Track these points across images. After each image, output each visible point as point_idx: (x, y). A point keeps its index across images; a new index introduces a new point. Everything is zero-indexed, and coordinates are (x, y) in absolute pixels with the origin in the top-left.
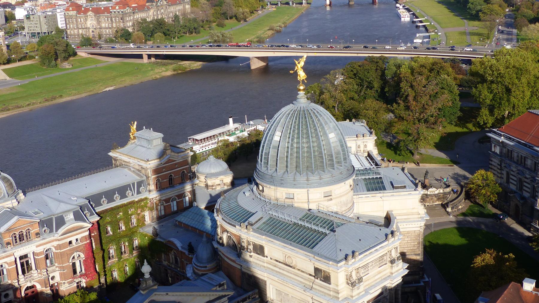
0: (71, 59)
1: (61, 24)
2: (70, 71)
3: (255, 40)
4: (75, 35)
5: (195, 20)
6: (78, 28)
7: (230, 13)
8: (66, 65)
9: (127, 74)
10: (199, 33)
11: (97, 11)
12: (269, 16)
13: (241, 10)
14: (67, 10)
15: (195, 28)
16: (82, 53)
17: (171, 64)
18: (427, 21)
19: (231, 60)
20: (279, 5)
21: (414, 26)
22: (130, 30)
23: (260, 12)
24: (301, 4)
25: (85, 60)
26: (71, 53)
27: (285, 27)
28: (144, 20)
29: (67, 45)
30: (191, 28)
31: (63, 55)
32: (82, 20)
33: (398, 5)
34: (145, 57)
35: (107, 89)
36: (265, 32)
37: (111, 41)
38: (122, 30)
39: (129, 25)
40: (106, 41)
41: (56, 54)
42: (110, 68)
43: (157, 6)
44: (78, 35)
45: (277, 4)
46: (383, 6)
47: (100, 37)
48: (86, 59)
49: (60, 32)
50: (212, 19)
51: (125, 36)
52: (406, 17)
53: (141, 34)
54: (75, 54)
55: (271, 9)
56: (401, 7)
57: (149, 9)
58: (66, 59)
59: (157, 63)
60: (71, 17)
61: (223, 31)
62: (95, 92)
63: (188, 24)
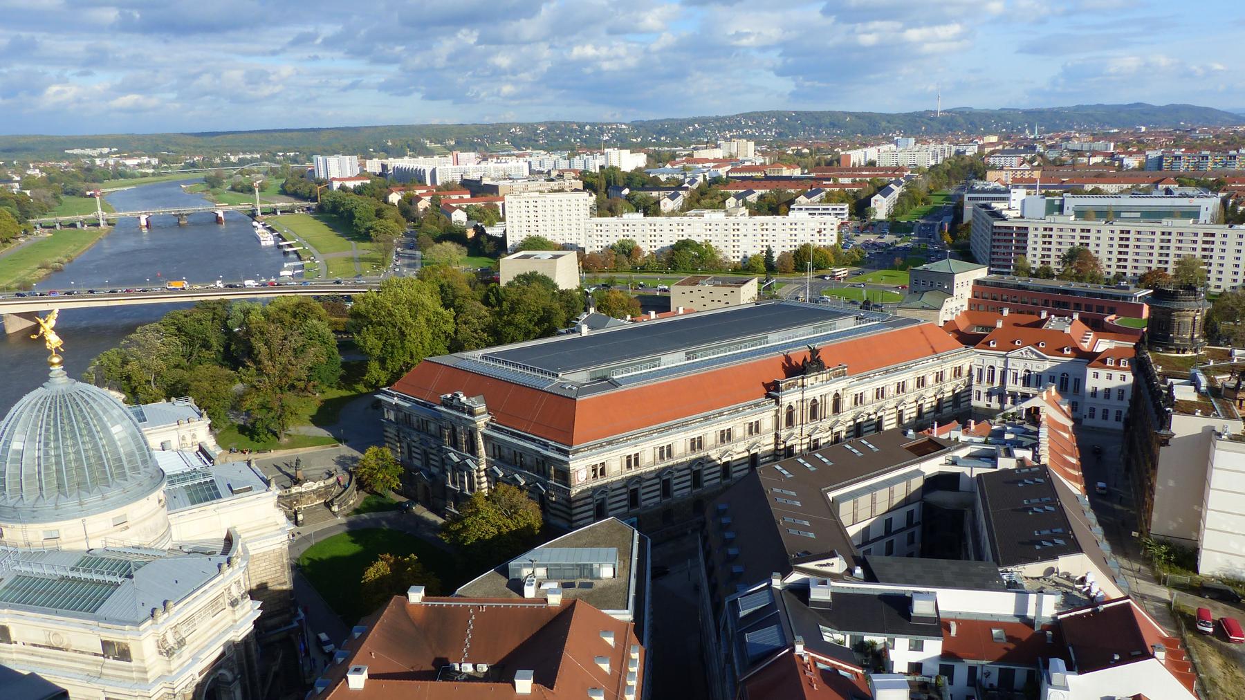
3: (13, 286)
12: (40, 246)
18: (298, 244)
20: (58, 227)
24: (98, 225)
27: (70, 262)
33: (255, 223)
36: (31, 272)
45: (54, 227)
46: (233, 226)
52: (267, 240)
56: (260, 226)
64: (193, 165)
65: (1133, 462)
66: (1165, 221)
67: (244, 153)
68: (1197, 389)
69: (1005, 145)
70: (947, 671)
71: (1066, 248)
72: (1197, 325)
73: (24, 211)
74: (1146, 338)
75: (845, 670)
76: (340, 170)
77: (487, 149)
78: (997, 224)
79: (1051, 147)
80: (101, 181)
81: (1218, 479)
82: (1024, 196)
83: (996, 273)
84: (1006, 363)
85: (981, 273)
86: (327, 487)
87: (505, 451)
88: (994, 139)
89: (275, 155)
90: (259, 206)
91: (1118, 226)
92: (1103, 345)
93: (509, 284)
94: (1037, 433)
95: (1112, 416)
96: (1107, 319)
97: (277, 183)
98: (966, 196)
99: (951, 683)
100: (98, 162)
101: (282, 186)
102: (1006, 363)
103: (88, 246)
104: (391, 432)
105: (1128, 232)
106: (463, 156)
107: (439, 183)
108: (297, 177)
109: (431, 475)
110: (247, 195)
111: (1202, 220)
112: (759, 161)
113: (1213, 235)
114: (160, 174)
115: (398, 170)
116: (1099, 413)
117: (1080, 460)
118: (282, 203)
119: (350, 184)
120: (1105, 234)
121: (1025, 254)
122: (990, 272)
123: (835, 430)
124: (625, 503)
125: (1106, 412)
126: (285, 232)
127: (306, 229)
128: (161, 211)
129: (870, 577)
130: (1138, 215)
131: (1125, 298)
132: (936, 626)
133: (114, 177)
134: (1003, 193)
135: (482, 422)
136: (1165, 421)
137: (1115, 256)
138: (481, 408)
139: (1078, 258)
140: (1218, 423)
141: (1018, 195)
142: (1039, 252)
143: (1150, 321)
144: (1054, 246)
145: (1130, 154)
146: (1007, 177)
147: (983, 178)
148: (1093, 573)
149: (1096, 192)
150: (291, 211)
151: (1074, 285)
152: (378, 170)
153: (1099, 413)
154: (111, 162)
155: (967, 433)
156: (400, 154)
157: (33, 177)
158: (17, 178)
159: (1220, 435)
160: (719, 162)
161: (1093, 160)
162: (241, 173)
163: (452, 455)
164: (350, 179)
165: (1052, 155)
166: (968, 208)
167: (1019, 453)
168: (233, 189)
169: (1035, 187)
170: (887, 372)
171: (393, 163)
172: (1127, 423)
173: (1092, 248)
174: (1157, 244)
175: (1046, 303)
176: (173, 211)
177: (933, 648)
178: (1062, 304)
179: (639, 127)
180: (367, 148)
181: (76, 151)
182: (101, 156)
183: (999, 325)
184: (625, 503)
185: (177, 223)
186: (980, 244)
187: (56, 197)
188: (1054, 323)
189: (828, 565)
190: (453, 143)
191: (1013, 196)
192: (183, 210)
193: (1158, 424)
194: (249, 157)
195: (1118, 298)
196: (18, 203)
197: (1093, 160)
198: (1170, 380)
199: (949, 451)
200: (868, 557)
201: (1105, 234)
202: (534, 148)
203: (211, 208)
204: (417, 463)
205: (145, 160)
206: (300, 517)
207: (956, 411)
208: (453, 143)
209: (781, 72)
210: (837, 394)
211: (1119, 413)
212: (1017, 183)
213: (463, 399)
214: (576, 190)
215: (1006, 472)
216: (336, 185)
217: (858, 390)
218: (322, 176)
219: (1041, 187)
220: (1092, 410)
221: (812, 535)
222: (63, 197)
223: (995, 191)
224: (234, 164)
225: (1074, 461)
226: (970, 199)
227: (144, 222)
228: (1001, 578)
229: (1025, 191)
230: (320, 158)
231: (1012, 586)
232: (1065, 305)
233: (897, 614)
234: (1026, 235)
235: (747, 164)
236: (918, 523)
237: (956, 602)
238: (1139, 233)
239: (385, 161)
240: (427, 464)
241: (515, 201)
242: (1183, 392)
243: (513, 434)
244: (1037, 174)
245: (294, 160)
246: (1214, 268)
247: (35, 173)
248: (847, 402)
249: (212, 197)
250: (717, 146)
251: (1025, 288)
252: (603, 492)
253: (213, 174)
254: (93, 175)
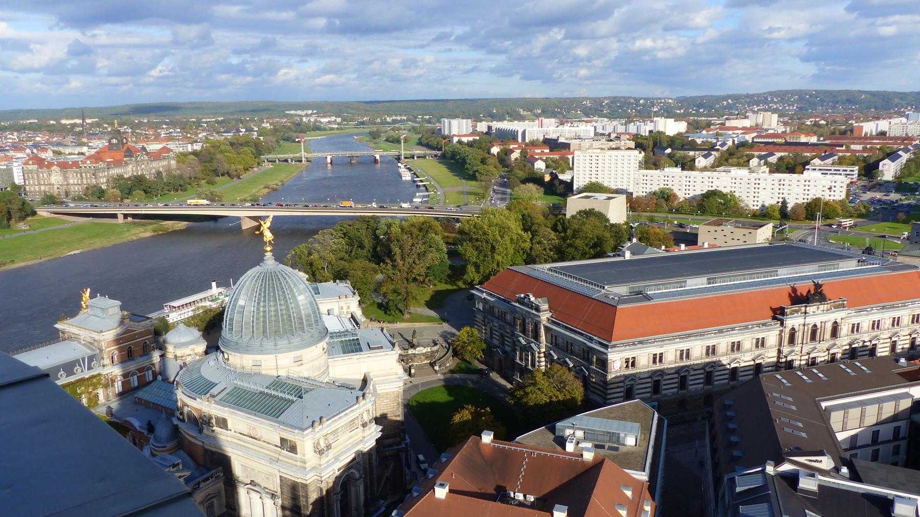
0: (29, 218)
1: (18, 180)
2: (27, 233)
4: (35, 192)
5: (181, 177)
6: (39, 184)
7: (221, 170)
8: (22, 226)
9: (97, 235)
10: (186, 190)
11: (64, 166)
12: (266, 173)
13: (233, 167)
14: (26, 163)
15: (180, 186)
16: (43, 212)
17: (151, 224)
18: (427, 180)
19: (220, 220)
21: (415, 185)
22: (104, 187)
23: (256, 169)
25: (46, 220)
26: (29, 212)
27: (282, 185)
28: (121, 177)
29: (24, 203)
30: (177, 185)
31: (18, 214)
32: (45, 175)
33: (399, 165)
34: (121, 217)
35: (72, 253)
36: (260, 190)
37: (80, 199)
38: (94, 186)
39: (103, 183)
40: (74, 200)
41: (9, 212)
42: (79, 228)
43: (137, 161)
44: (40, 192)
47: (67, 194)
48: (48, 218)
49: (16, 188)
50: (200, 175)
51: (99, 194)
53: (117, 192)
54: (34, 213)
55: (268, 166)
57: (127, 164)
58: (22, 219)
59: (134, 223)
60: (31, 172)
61: (212, 188)
62: (57, 256)
63: (172, 181)
64: (363, 123)
67: (396, 115)
73: (259, 150)
76: (459, 129)
77: (564, 117)
80: (305, 133)
86: (432, 352)
87: (560, 341)
89: (416, 118)
90: (403, 153)
93: (573, 217)
97: (416, 137)
100: (304, 119)
101: (419, 139)
103: (294, 174)
104: (479, 317)
106: (546, 121)
107: (527, 141)
108: (429, 134)
109: (505, 352)
110: (396, 145)
112: (781, 129)
114: (341, 129)
115: (498, 130)
118: (419, 151)
119: (465, 140)
123: (832, 351)
124: (676, 385)
126: (418, 172)
127: (433, 170)
128: (340, 153)
129: (855, 476)
133: (313, 130)
135: (545, 317)
138: (545, 307)
150: (424, 157)
152: (485, 130)
154: (312, 120)
156: (501, 119)
157: (265, 128)
158: (256, 129)
160: (747, 130)
162: (393, 129)
163: (521, 339)
164: (465, 136)
168: (387, 140)
170: (883, 308)
171: (496, 125)
176: (348, 154)
179: (683, 102)
180: (479, 114)
181: (292, 112)
182: (307, 115)
184: (676, 385)
185: (349, 162)
187: (277, 141)
189: (816, 461)
190: (539, 111)
192: (354, 153)
194: (399, 118)
196: (255, 145)
200: (854, 460)
202: (599, 117)
203: (372, 153)
204: (496, 342)
205: (333, 118)
206: (413, 371)
208: (539, 111)
209: (806, 59)
210: (836, 322)
213: (533, 299)
214: (629, 149)
216: (456, 139)
217: (855, 321)
218: (447, 133)
221: (804, 435)
222: (281, 142)
224: (389, 123)
227: (329, 161)
230: (446, 120)
235: (770, 132)
236: (903, 438)
239: (490, 124)
240: (503, 344)
241: (581, 156)
243: (566, 328)
245: (429, 122)
247: (266, 125)
248: (845, 329)
249: (373, 145)
250: (746, 117)
252: (660, 375)
253: (375, 129)
254: (301, 128)
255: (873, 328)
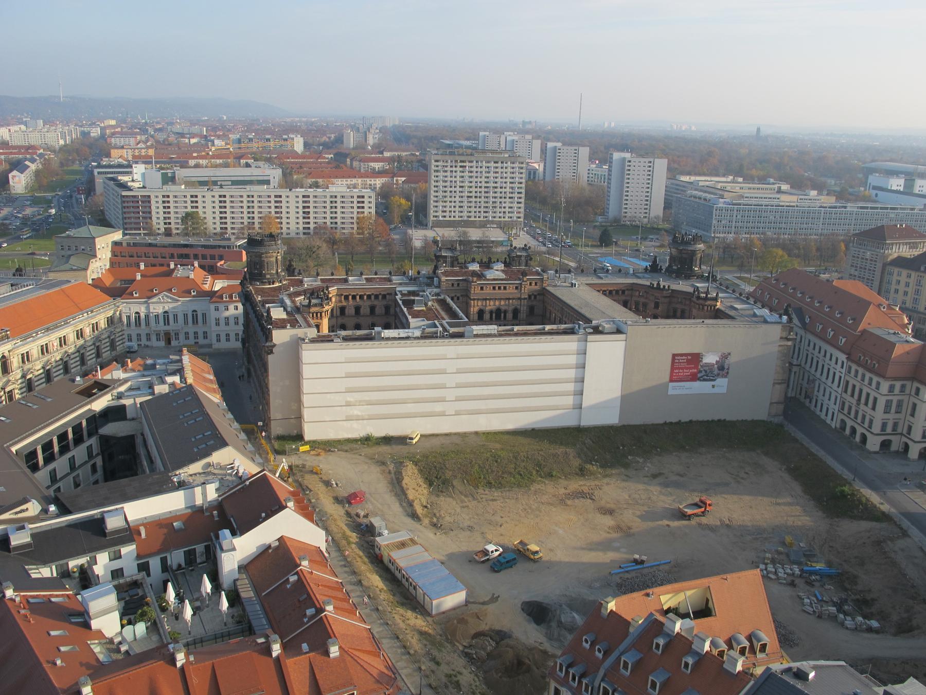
65: (252, 370)
66: (248, 187)
68: (285, 310)
69: (122, 128)
70: (144, 567)
71: (182, 211)
72: (279, 263)
74: (247, 276)
75: (57, 596)
78: (124, 193)
79: (160, 130)
81: (307, 371)
82: (144, 171)
83: (130, 234)
84: (148, 308)
85: (117, 236)
88: (113, 122)
91: (217, 192)
92: (219, 285)
94: (181, 361)
95: (233, 337)
96: (219, 265)
98: (96, 171)
99: (149, 575)
102: (148, 308)
105: (225, 196)
111: (272, 186)
113: (280, 196)
116: (223, 338)
117: (216, 375)
120: (209, 199)
121: (151, 218)
122: (124, 234)
123: (7, 389)
125: (228, 335)
129: (64, 510)
130: (230, 183)
131: (229, 247)
132: (128, 534)
134: (127, 167)
136: (268, 336)
137: (218, 215)
139: (189, 218)
140: (299, 332)
141: (139, 170)
142: (161, 215)
143: (250, 264)
144: (172, 210)
145: (219, 137)
146: (128, 154)
147: (108, 155)
148: (235, 459)
149: (197, 166)
151: (191, 241)
153: (223, 338)
155: (126, 371)
159: (304, 340)
161: (193, 141)
165: (161, 137)
166: (99, 181)
167: (170, 379)
169: (151, 163)
170: (48, 329)
172: (244, 342)
173: (200, 210)
174: (245, 204)
175: (172, 256)
177: (128, 550)
178: (185, 255)
183: (139, 277)
186: (113, 214)
188: (180, 272)
189: (20, 512)
191: (135, 170)
193: (264, 339)
195: (224, 247)
197: (193, 141)
198: (267, 305)
199: (114, 388)
200: (58, 495)
201: (209, 199)
207: (114, 353)
211: (237, 335)
212: (137, 159)
215: (163, 396)
217: (24, 350)
219: (156, 163)
220: (218, 336)
223: (120, 166)
225: (212, 377)
226: (99, 173)
228: (173, 482)
229: (143, 166)
231: (181, 485)
232: (187, 256)
233: (96, 534)
234: (149, 202)
236: (97, 455)
237: (140, 510)
238: (232, 196)
242: (277, 313)
244: (151, 152)
246: (284, 221)
248: (15, 362)
251: (156, 246)
255: (43, 353)
